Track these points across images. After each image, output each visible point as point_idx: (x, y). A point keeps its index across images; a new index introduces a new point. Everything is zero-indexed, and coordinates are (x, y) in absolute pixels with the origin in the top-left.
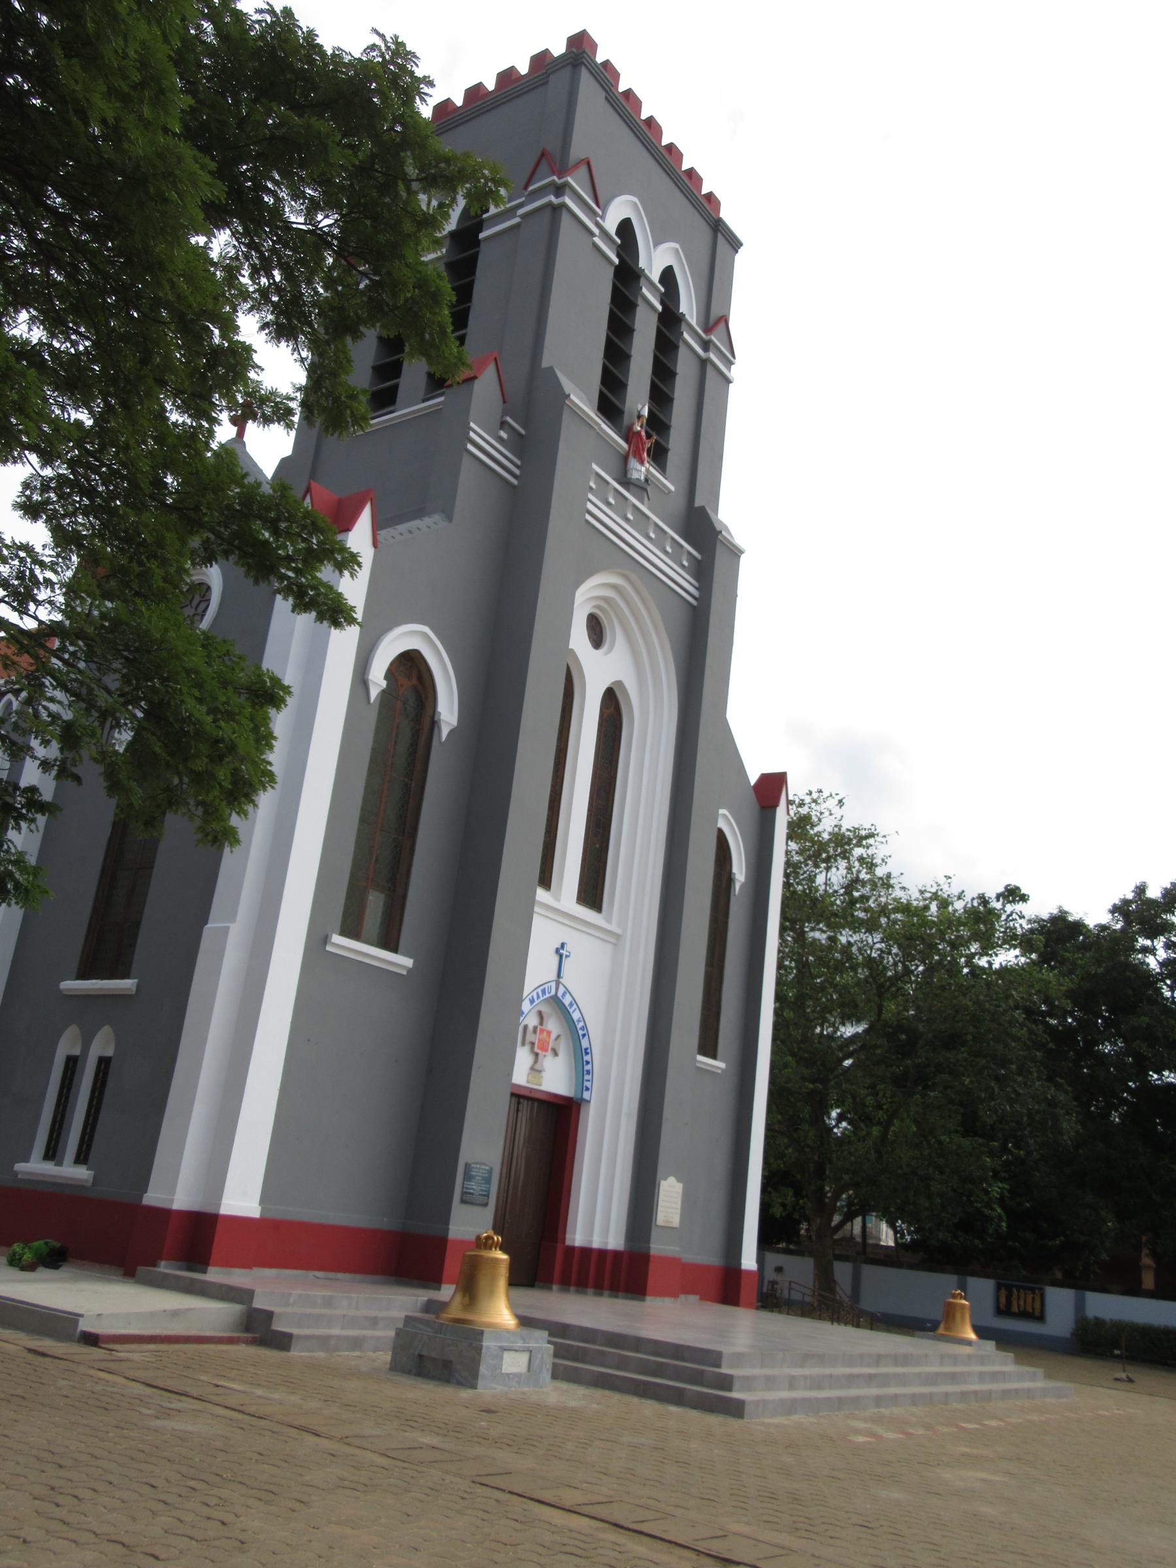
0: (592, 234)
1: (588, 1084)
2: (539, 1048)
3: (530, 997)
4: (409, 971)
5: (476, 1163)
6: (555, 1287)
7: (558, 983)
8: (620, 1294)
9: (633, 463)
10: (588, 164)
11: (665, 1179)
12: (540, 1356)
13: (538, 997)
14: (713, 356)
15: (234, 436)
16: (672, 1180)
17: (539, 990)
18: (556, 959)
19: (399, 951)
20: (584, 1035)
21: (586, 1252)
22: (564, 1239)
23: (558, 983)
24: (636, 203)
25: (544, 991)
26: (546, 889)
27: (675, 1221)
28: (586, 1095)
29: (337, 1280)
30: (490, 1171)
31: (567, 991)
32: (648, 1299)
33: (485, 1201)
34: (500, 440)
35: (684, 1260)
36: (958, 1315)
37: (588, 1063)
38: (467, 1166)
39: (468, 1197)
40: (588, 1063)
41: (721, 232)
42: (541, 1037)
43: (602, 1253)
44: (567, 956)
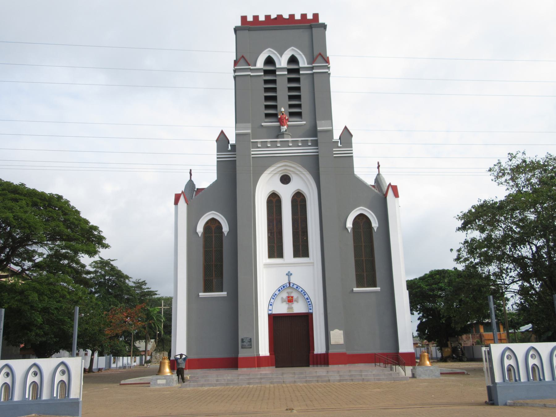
0: (249, 75)
1: (311, 308)
2: (288, 302)
3: (278, 289)
4: (227, 294)
5: (245, 338)
6: (310, 366)
7: (290, 283)
8: (326, 365)
9: (282, 127)
10: (243, 57)
11: (333, 331)
12: (169, 380)
13: (282, 289)
14: (314, 71)
15: (189, 179)
16: (336, 331)
17: (282, 287)
18: (287, 276)
19: (224, 290)
20: (305, 295)
21: (317, 355)
22: (313, 353)
23: (290, 283)
24: (270, 50)
25: (284, 287)
26: (282, 258)
27: (341, 341)
28: (311, 311)
29: (220, 370)
30: (251, 339)
31: (294, 284)
32: (330, 366)
33: (242, 347)
34: (229, 151)
35: (347, 354)
36: (423, 358)
37: (309, 302)
39: (243, 347)
40: (309, 302)
41: (313, 27)
42: (289, 299)
43: (320, 355)
44: (290, 275)
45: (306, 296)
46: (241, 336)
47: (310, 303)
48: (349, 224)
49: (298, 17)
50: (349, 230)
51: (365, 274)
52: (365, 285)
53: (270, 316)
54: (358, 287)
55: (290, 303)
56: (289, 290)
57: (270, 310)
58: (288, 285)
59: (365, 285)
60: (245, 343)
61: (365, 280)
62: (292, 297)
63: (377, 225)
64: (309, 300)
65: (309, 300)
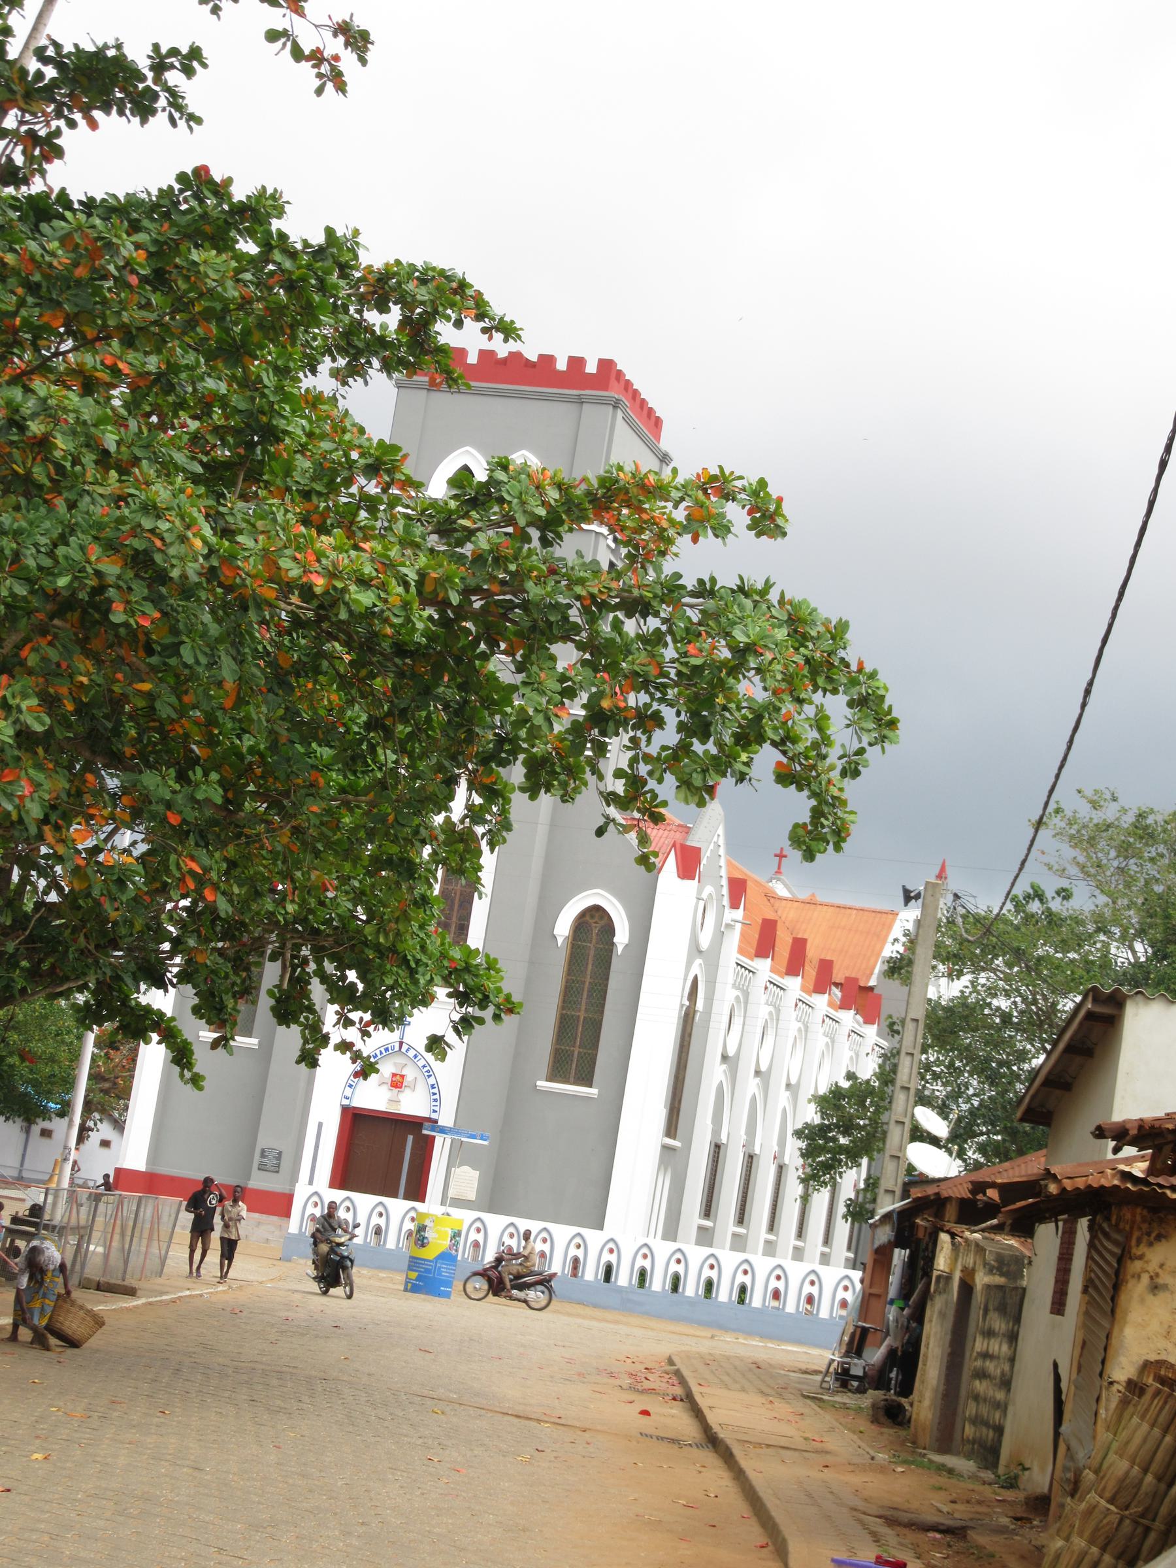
1: (437, 1109)
4: (260, 1043)
7: (401, 1043)
23: (401, 1043)
25: (387, 1050)
30: (280, 1153)
31: (410, 1047)
37: (434, 1094)
38: (263, 1151)
40: (434, 1094)
45: (432, 1081)
46: (262, 1142)
47: (437, 1097)
48: (563, 927)
49: (562, 365)
50: (560, 941)
51: (576, 1053)
52: (572, 1079)
53: (346, 1110)
54: (549, 1079)
55: (395, 1091)
56: (400, 1060)
57: (347, 1098)
58: (397, 1048)
59: (572, 1079)
60: (266, 1160)
61: (574, 1066)
62: (403, 1077)
63: (626, 941)
64: (436, 1091)
65: (436, 1091)
